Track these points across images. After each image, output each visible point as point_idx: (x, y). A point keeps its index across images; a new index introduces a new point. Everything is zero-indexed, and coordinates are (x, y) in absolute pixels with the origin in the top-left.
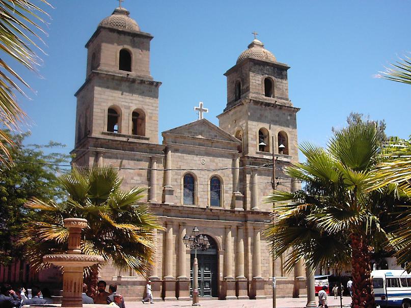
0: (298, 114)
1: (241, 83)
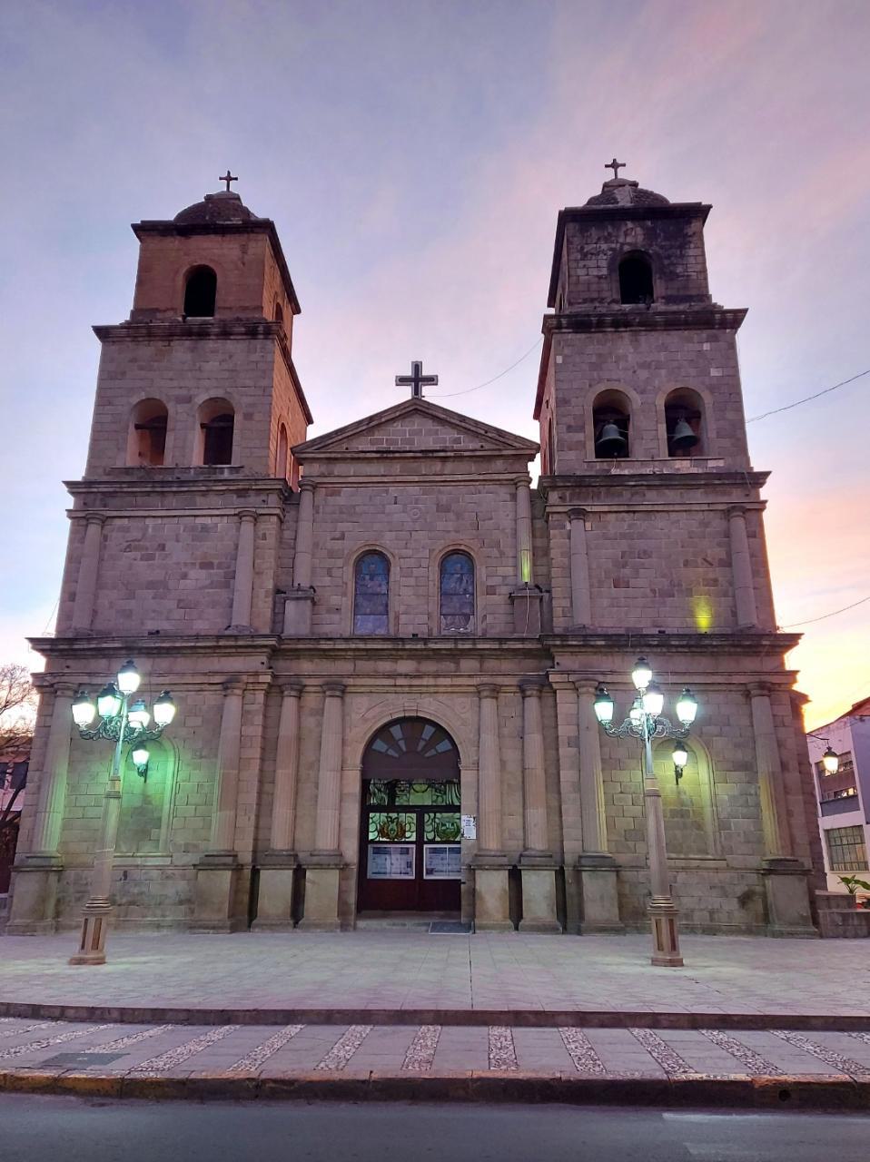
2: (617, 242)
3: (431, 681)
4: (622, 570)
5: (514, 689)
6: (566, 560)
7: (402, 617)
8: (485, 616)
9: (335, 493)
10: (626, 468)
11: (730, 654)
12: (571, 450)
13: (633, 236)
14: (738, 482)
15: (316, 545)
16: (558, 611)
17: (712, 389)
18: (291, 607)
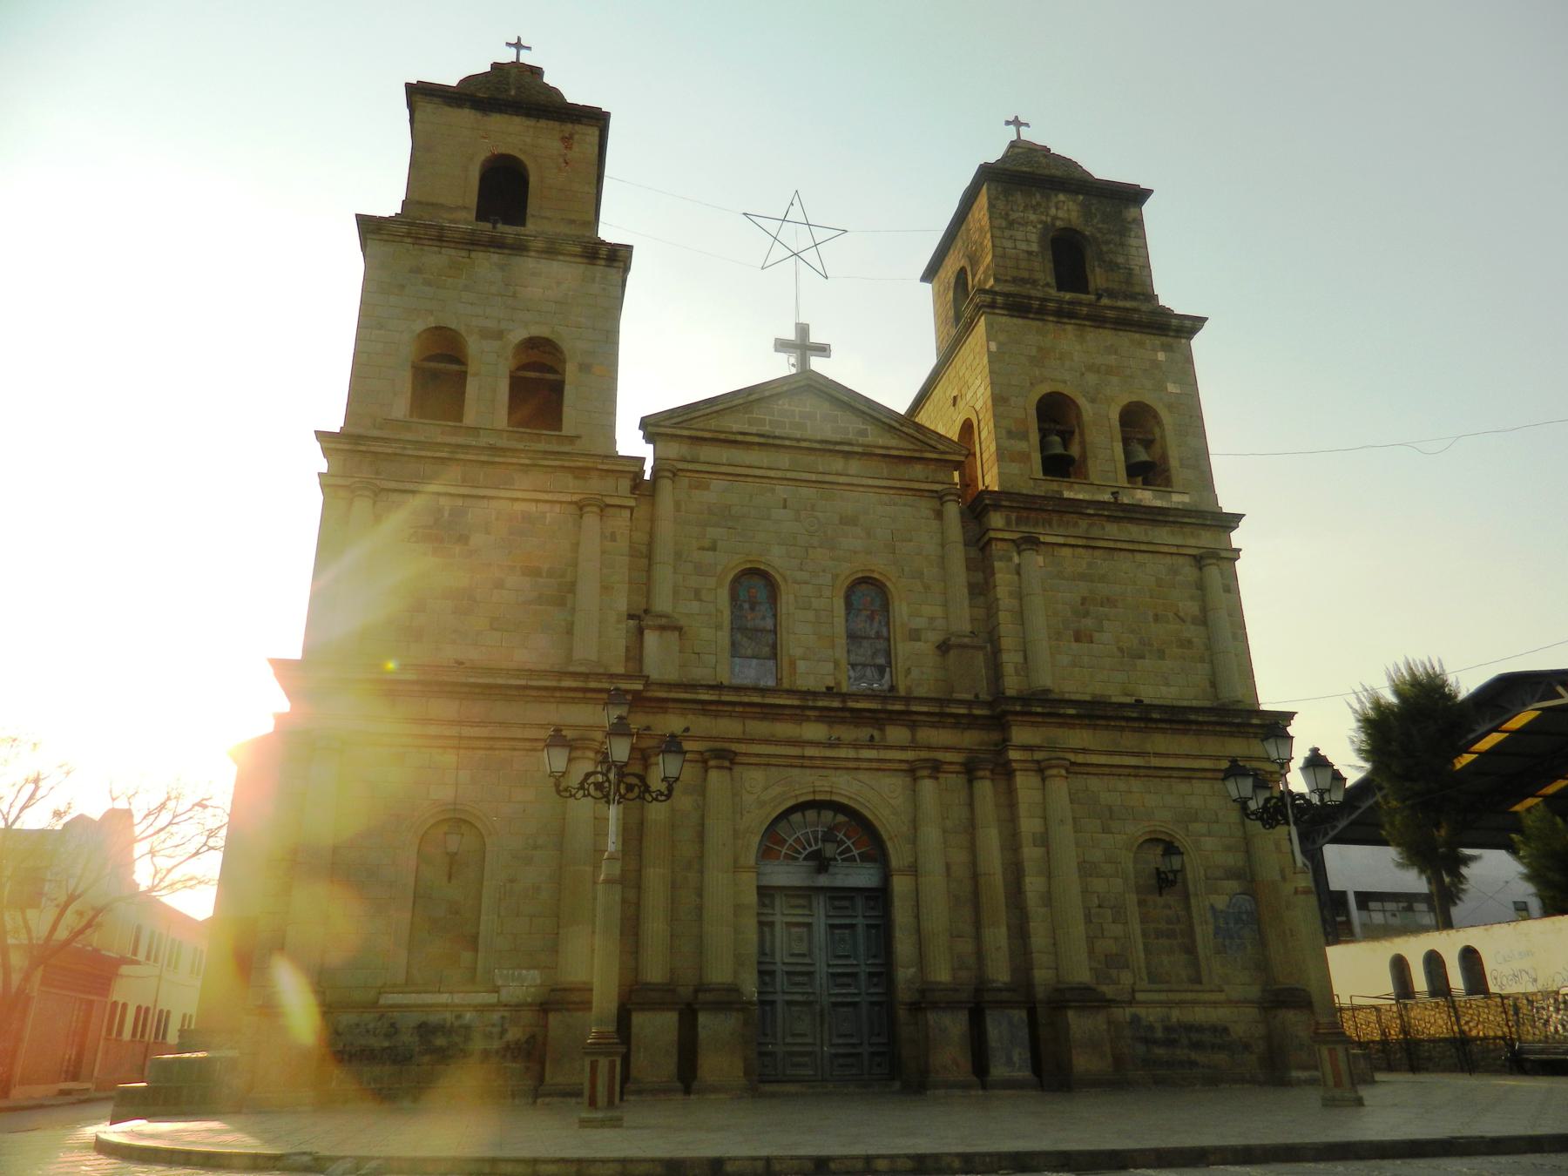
0: (1198, 344)
2: (1047, 215)
3: (852, 754)
4: (1083, 620)
5: (958, 768)
6: (1015, 602)
7: (798, 662)
8: (909, 669)
10: (1079, 492)
11: (1215, 733)
12: (1013, 462)
13: (1066, 210)
14: (1209, 522)
15: (678, 555)
16: (1009, 669)
17: (1170, 407)
18: (651, 638)
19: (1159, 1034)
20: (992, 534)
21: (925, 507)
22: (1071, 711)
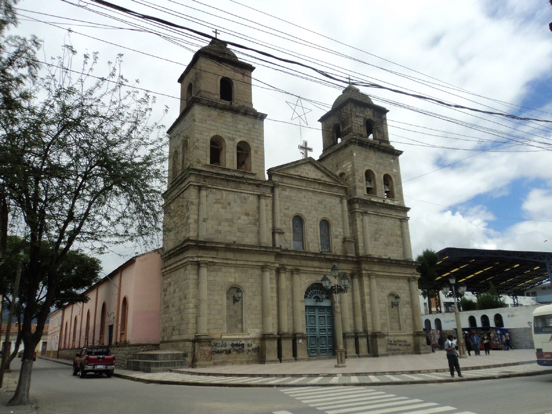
0: (400, 157)
1: (341, 126)
7: (310, 244)
9: (284, 190)
13: (369, 114)
18: (277, 236)
19: (393, 343)
20: (357, 210)
21: (337, 200)
22: (376, 260)
